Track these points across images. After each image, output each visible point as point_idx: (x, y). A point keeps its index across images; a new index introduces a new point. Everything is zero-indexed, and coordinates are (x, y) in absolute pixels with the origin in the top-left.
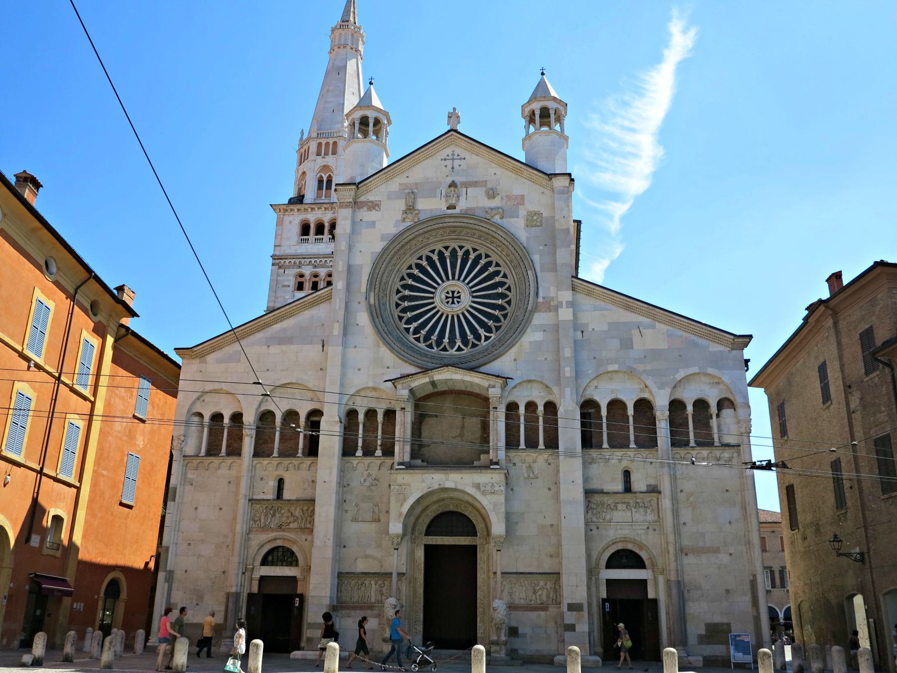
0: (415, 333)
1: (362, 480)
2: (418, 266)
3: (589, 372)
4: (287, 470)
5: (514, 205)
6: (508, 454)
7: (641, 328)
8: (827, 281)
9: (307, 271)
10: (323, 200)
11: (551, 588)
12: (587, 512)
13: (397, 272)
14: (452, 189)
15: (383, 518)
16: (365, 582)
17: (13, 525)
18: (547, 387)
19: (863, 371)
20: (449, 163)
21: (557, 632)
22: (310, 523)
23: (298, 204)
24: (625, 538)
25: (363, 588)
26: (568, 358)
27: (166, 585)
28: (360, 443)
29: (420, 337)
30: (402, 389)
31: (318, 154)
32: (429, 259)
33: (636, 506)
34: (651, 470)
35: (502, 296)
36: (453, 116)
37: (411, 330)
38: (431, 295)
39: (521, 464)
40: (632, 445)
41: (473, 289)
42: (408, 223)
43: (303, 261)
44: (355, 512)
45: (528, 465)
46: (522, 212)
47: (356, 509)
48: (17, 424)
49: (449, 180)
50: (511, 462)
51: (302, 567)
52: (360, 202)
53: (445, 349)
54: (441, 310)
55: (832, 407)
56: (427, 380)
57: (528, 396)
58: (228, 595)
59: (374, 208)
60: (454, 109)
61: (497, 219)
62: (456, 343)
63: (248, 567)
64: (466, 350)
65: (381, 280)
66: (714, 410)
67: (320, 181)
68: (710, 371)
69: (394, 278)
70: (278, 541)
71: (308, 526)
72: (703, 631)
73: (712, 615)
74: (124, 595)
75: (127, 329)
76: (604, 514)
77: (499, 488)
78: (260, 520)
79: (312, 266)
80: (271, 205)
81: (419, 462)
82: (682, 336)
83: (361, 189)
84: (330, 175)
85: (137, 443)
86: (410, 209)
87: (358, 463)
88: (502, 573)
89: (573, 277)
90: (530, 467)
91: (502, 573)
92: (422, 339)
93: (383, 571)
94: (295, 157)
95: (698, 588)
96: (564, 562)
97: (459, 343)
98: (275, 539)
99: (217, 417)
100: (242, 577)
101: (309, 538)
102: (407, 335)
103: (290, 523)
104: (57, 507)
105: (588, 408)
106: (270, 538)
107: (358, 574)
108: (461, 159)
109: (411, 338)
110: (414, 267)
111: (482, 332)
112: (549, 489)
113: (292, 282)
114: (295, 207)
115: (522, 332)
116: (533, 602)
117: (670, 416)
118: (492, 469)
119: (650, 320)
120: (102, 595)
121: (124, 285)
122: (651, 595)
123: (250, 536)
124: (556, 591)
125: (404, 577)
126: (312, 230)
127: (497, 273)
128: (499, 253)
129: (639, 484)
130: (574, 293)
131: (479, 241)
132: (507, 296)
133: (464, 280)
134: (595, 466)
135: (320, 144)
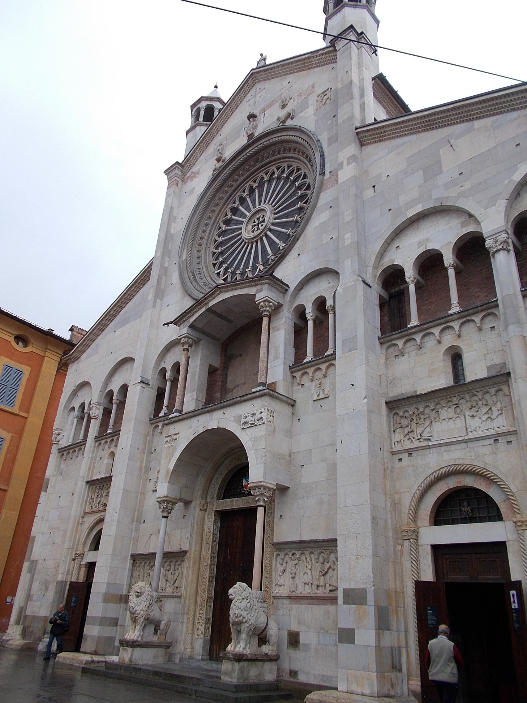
6: (294, 374)
13: (213, 224)
27: (29, 575)
29: (227, 276)
34: (491, 339)
45: (318, 382)
56: (203, 310)
60: (262, 55)
62: (257, 268)
76: (419, 430)
77: (260, 416)
83: (185, 167)
86: (218, 160)
100: (70, 563)
125: (186, 556)
131: (279, 156)
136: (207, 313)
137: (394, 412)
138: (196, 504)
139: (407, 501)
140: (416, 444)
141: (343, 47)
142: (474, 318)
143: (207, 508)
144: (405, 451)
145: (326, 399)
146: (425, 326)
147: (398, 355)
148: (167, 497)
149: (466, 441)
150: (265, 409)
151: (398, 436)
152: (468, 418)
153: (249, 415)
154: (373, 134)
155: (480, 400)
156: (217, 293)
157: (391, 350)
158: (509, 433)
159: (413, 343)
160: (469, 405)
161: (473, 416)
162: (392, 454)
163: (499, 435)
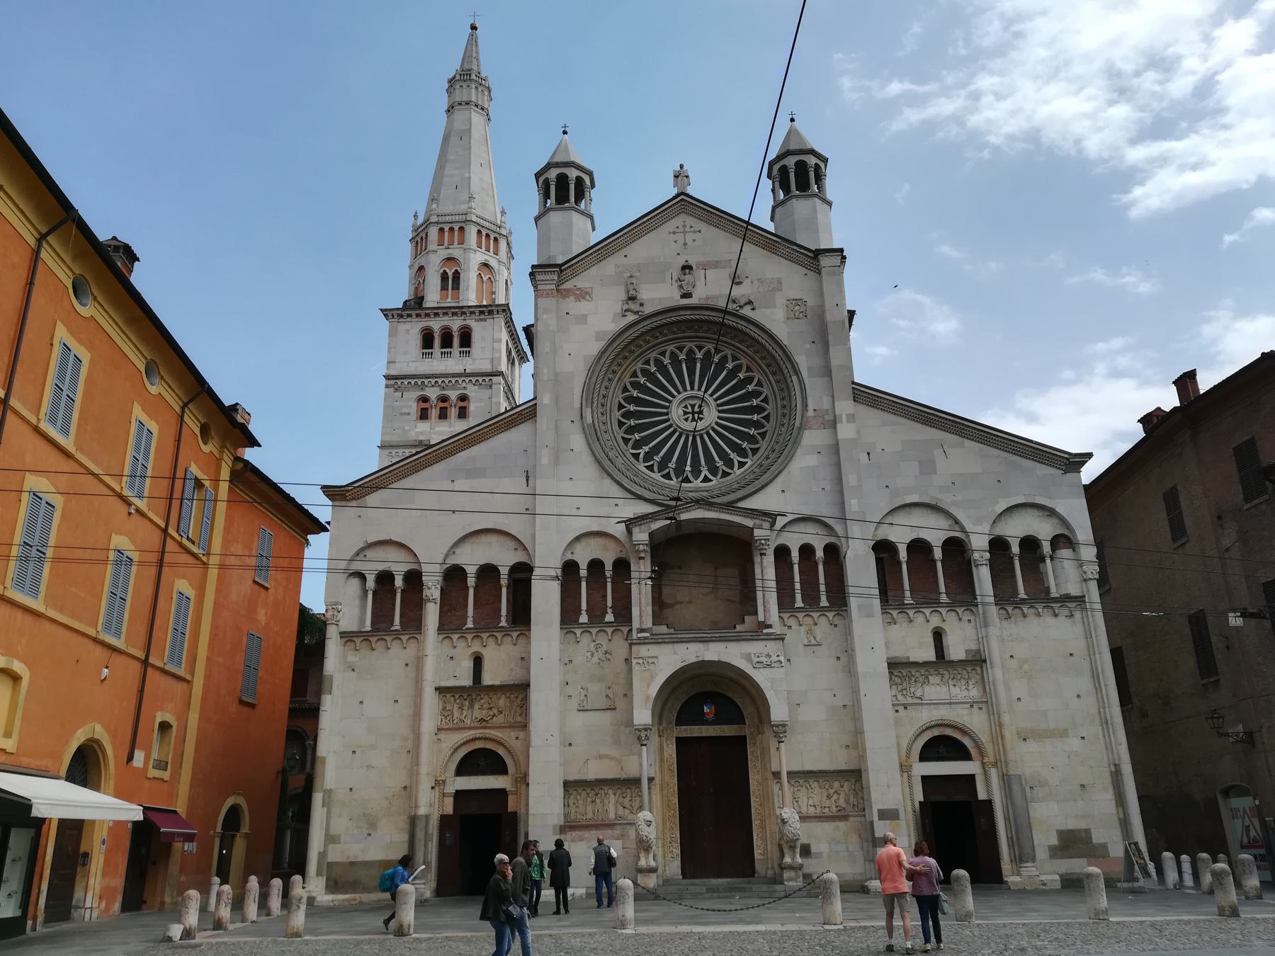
1: (589, 654)
2: (645, 373)
4: (485, 646)
5: (769, 291)
7: (945, 447)
8: (1173, 383)
9: (433, 394)
10: (449, 302)
11: (849, 790)
14: (687, 271)
15: (620, 705)
16: (600, 792)
17: (113, 735)
18: (826, 525)
19: (1241, 496)
20: (680, 237)
21: (862, 848)
22: (521, 715)
23: (413, 309)
24: (942, 720)
25: (598, 801)
28: (584, 606)
31: (441, 244)
32: (658, 363)
33: (954, 678)
34: (969, 630)
35: (759, 409)
36: (680, 176)
37: (641, 456)
38: (666, 411)
40: (944, 598)
41: (718, 402)
42: (631, 318)
43: (426, 381)
44: (582, 699)
45: (807, 629)
46: (780, 300)
47: (583, 693)
48: (116, 595)
49: (681, 261)
50: (785, 626)
51: (512, 775)
52: (564, 290)
53: (687, 480)
54: (679, 429)
55: (1188, 546)
57: (802, 538)
58: (413, 820)
59: (584, 298)
60: (681, 166)
61: (746, 311)
63: (438, 779)
64: (715, 481)
65: (599, 391)
66: (1046, 548)
67: (444, 277)
68: (1039, 500)
69: (615, 390)
70: (477, 742)
71: (519, 719)
72: (1054, 841)
73: (1066, 819)
74: (245, 829)
75: (247, 463)
77: (777, 659)
78: (453, 714)
79: (438, 388)
80: (381, 310)
81: (663, 629)
82: (999, 455)
84: (456, 270)
85: (259, 618)
86: (632, 298)
87: (582, 632)
88: (789, 773)
90: (810, 630)
91: (789, 773)
92: (656, 468)
93: (623, 776)
94: (408, 248)
95: (1043, 784)
96: (869, 754)
97: (705, 472)
98: (474, 740)
99: (385, 578)
101: (521, 735)
102: (636, 462)
103: (493, 716)
104: (162, 709)
105: (883, 550)
106: (468, 738)
107: (590, 781)
108: (695, 232)
110: (639, 374)
111: (733, 456)
112: (838, 658)
113: (414, 408)
114: (413, 313)
115: (790, 458)
116: (827, 810)
117: (989, 560)
118: (767, 634)
119: (955, 436)
120: (219, 829)
121: (237, 404)
122: (982, 796)
123: (439, 737)
124: (856, 795)
125: (653, 783)
126: (437, 342)
127: (749, 380)
128: (751, 353)
129: (956, 651)
130: (856, 403)
132: (764, 410)
135: (442, 230)
139: (904, 744)
140: (910, 700)
142: (957, 609)
145: (818, 647)
146: (919, 606)
149: (950, 703)
152: (951, 685)
154: (868, 398)
155: (959, 674)
156: (694, 508)
158: (982, 702)
159: (904, 614)
160: (952, 676)
161: (955, 685)
163: (974, 702)
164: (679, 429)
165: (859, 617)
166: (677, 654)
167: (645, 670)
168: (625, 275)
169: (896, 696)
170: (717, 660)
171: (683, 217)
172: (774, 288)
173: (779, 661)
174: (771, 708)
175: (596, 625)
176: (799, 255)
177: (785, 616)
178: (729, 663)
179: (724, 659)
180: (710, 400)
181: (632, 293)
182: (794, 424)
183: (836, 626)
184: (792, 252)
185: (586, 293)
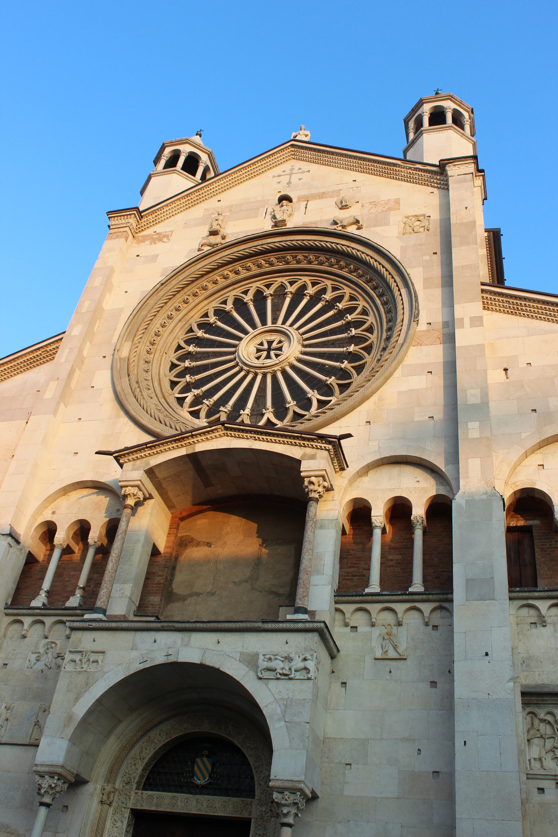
0: (192, 405)
3: (524, 435)
5: (383, 211)
6: (340, 606)
12: (528, 741)
14: (284, 202)
26: (474, 406)
28: (46, 585)
30: (132, 470)
37: (188, 401)
39: (368, 629)
41: (305, 336)
45: (384, 631)
46: (396, 218)
50: (346, 625)
56: (182, 452)
62: (263, 415)
77: (301, 665)
86: (214, 233)
89: (483, 284)
102: (180, 408)
109: (184, 413)
112: (433, 684)
133: (292, 325)
134: (547, 631)
136: (187, 459)
137: (528, 710)
138: (95, 789)
141: (458, 175)
143: (113, 801)
144: (551, 777)
145: (402, 662)
147: (535, 623)
148: (62, 767)
150: (312, 655)
151: (535, 751)
153: (278, 657)
157: (525, 612)
162: (528, 778)
164: (245, 368)
165: (467, 600)
166: (136, 649)
167: (80, 672)
168: (213, 216)
169: (540, 759)
170: (197, 662)
171: (293, 162)
172: (389, 208)
173: (306, 669)
174: (275, 754)
175: (51, 612)
176: (423, 174)
177: (349, 608)
178: (218, 670)
179: (212, 661)
180: (295, 335)
181: (215, 227)
182: (397, 341)
183: (435, 627)
184: (414, 172)
185: (165, 236)
